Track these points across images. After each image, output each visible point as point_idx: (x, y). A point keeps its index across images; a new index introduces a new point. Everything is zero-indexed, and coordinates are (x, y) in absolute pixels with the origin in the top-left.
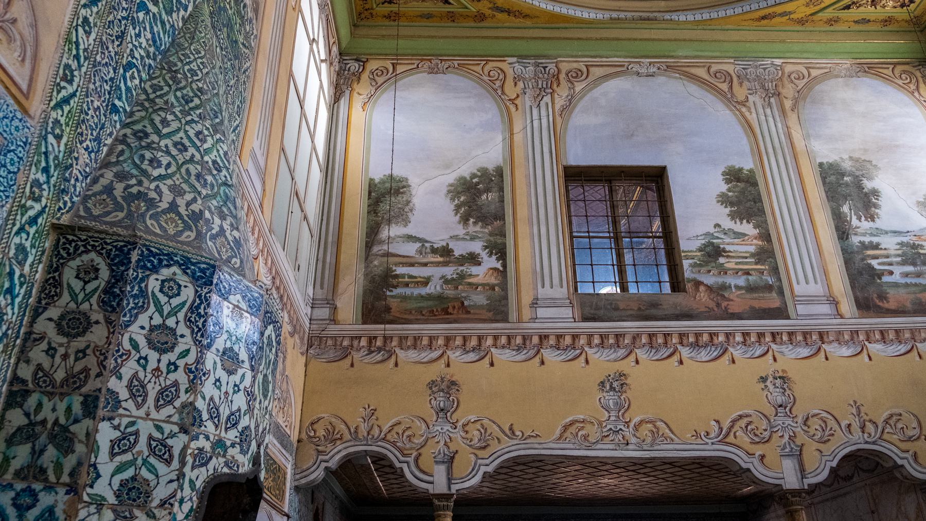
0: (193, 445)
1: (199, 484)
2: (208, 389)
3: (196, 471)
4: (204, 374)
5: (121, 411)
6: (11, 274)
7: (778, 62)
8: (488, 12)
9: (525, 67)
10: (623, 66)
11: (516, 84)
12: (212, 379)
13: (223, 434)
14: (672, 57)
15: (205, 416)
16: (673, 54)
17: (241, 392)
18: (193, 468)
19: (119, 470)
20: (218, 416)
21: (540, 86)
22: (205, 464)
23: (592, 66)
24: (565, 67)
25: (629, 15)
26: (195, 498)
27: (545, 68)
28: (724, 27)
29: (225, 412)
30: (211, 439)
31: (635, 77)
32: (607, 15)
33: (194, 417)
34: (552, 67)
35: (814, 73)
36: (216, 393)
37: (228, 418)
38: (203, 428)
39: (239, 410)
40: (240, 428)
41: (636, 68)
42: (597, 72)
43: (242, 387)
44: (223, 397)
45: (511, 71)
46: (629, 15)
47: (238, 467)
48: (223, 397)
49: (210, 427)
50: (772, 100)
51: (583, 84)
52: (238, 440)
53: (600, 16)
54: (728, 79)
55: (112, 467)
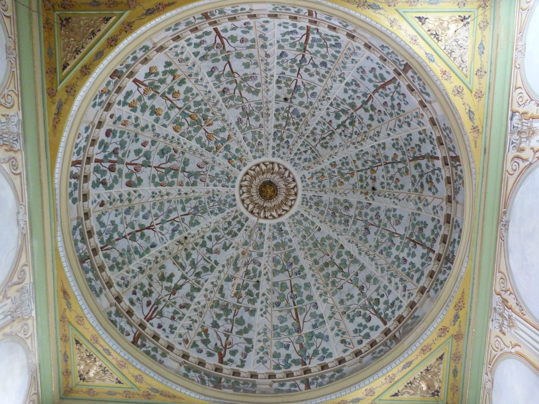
7: (34, 314)
8: (57, 99)
9: (16, 125)
10: (23, 201)
11: (3, 115)
14: (31, 237)
16: (34, 236)
21: (4, 135)
23: (21, 178)
24: (18, 156)
25: (58, 202)
27: (16, 140)
28: (55, 269)
31: (16, 211)
32: (57, 186)
34: (17, 146)
35: (29, 341)
41: (22, 211)
42: (17, 181)
45: (12, 114)
46: (58, 202)
50: (9, 317)
51: (8, 170)
53: (57, 181)
54: (20, 281)
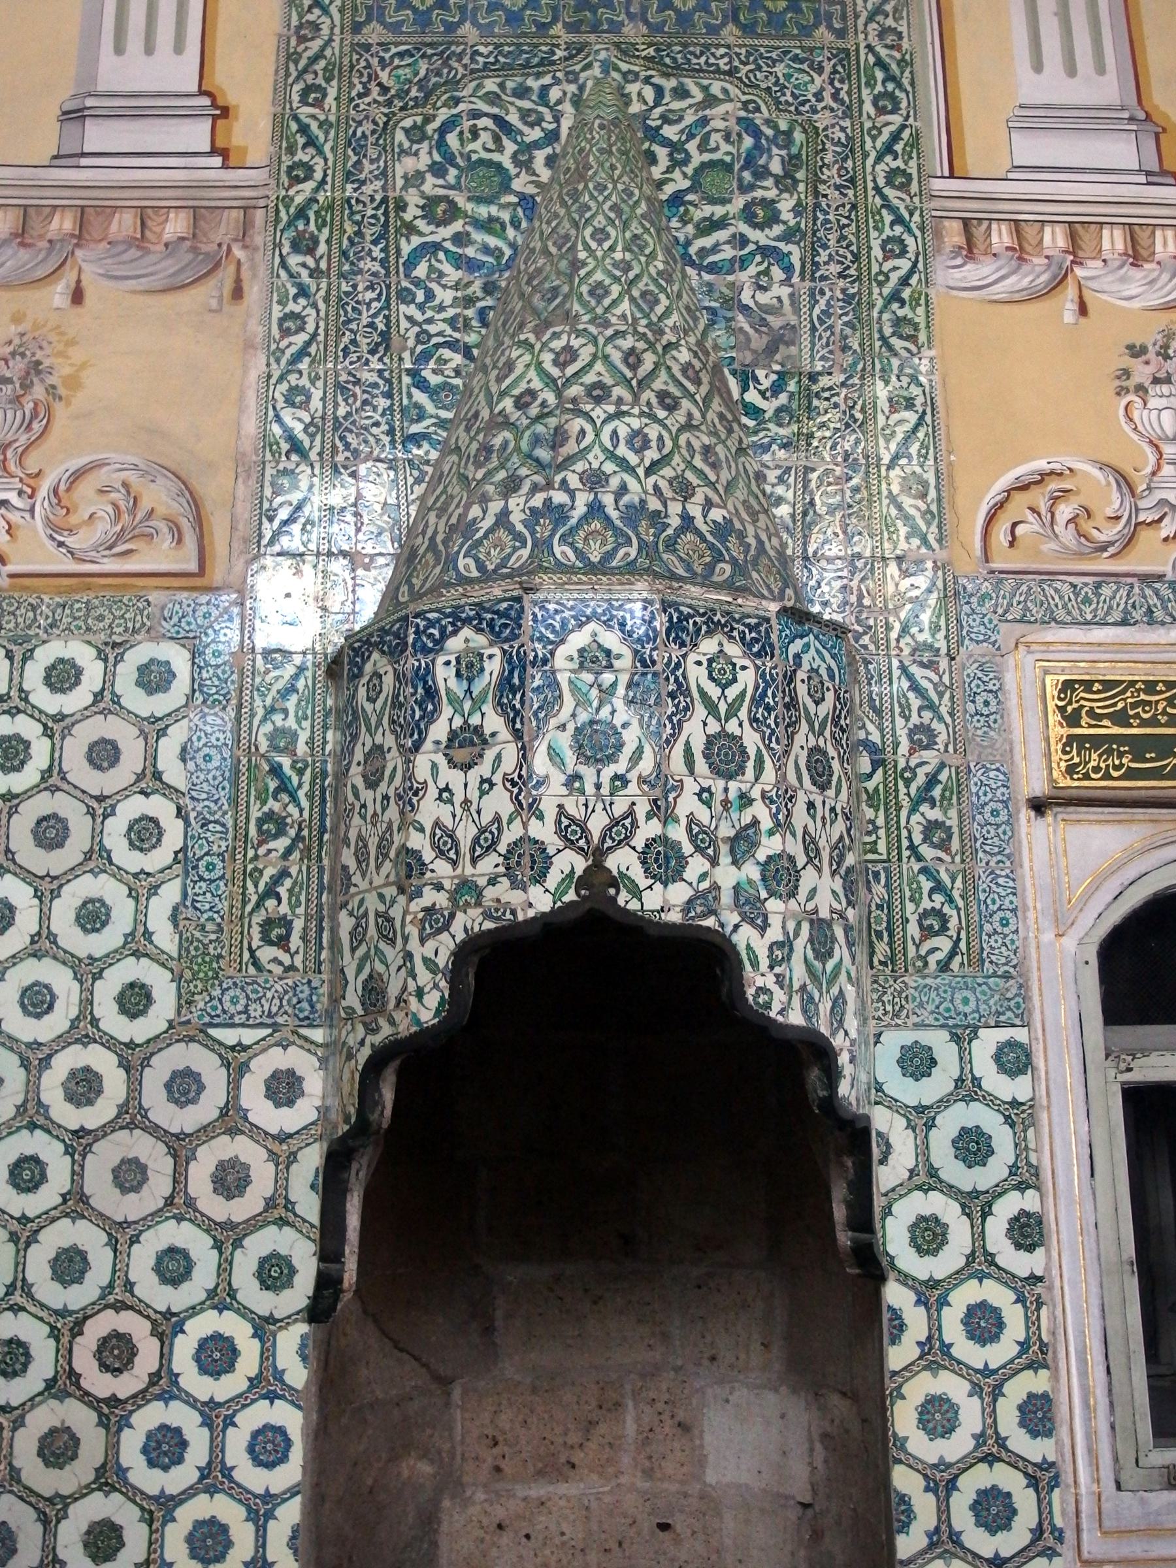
0: (415, 906)
1: (442, 960)
2: (429, 810)
3: (431, 944)
4: (416, 794)
5: (353, 890)
6: (276, 770)
12: (432, 792)
13: (469, 870)
15: (428, 855)
17: (499, 789)
18: (422, 941)
19: (360, 969)
20: (456, 844)
22: (446, 927)
26: (443, 984)
29: (466, 833)
30: (447, 884)
33: (409, 865)
36: (444, 813)
37: (476, 841)
38: (428, 875)
39: (497, 819)
40: (502, 848)
43: (497, 778)
44: (459, 811)
47: (513, 912)
48: (459, 811)
49: (442, 868)
52: (502, 869)
55: (354, 966)
